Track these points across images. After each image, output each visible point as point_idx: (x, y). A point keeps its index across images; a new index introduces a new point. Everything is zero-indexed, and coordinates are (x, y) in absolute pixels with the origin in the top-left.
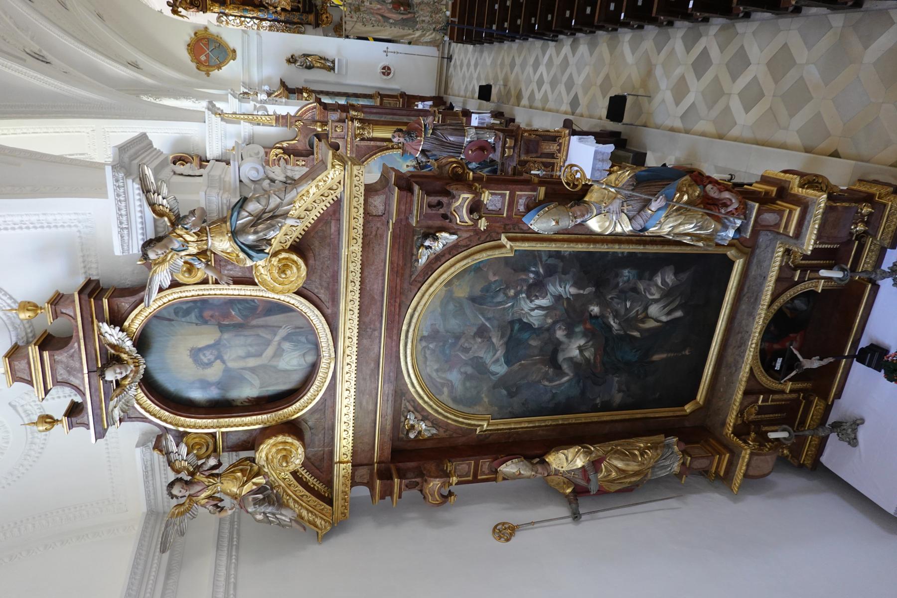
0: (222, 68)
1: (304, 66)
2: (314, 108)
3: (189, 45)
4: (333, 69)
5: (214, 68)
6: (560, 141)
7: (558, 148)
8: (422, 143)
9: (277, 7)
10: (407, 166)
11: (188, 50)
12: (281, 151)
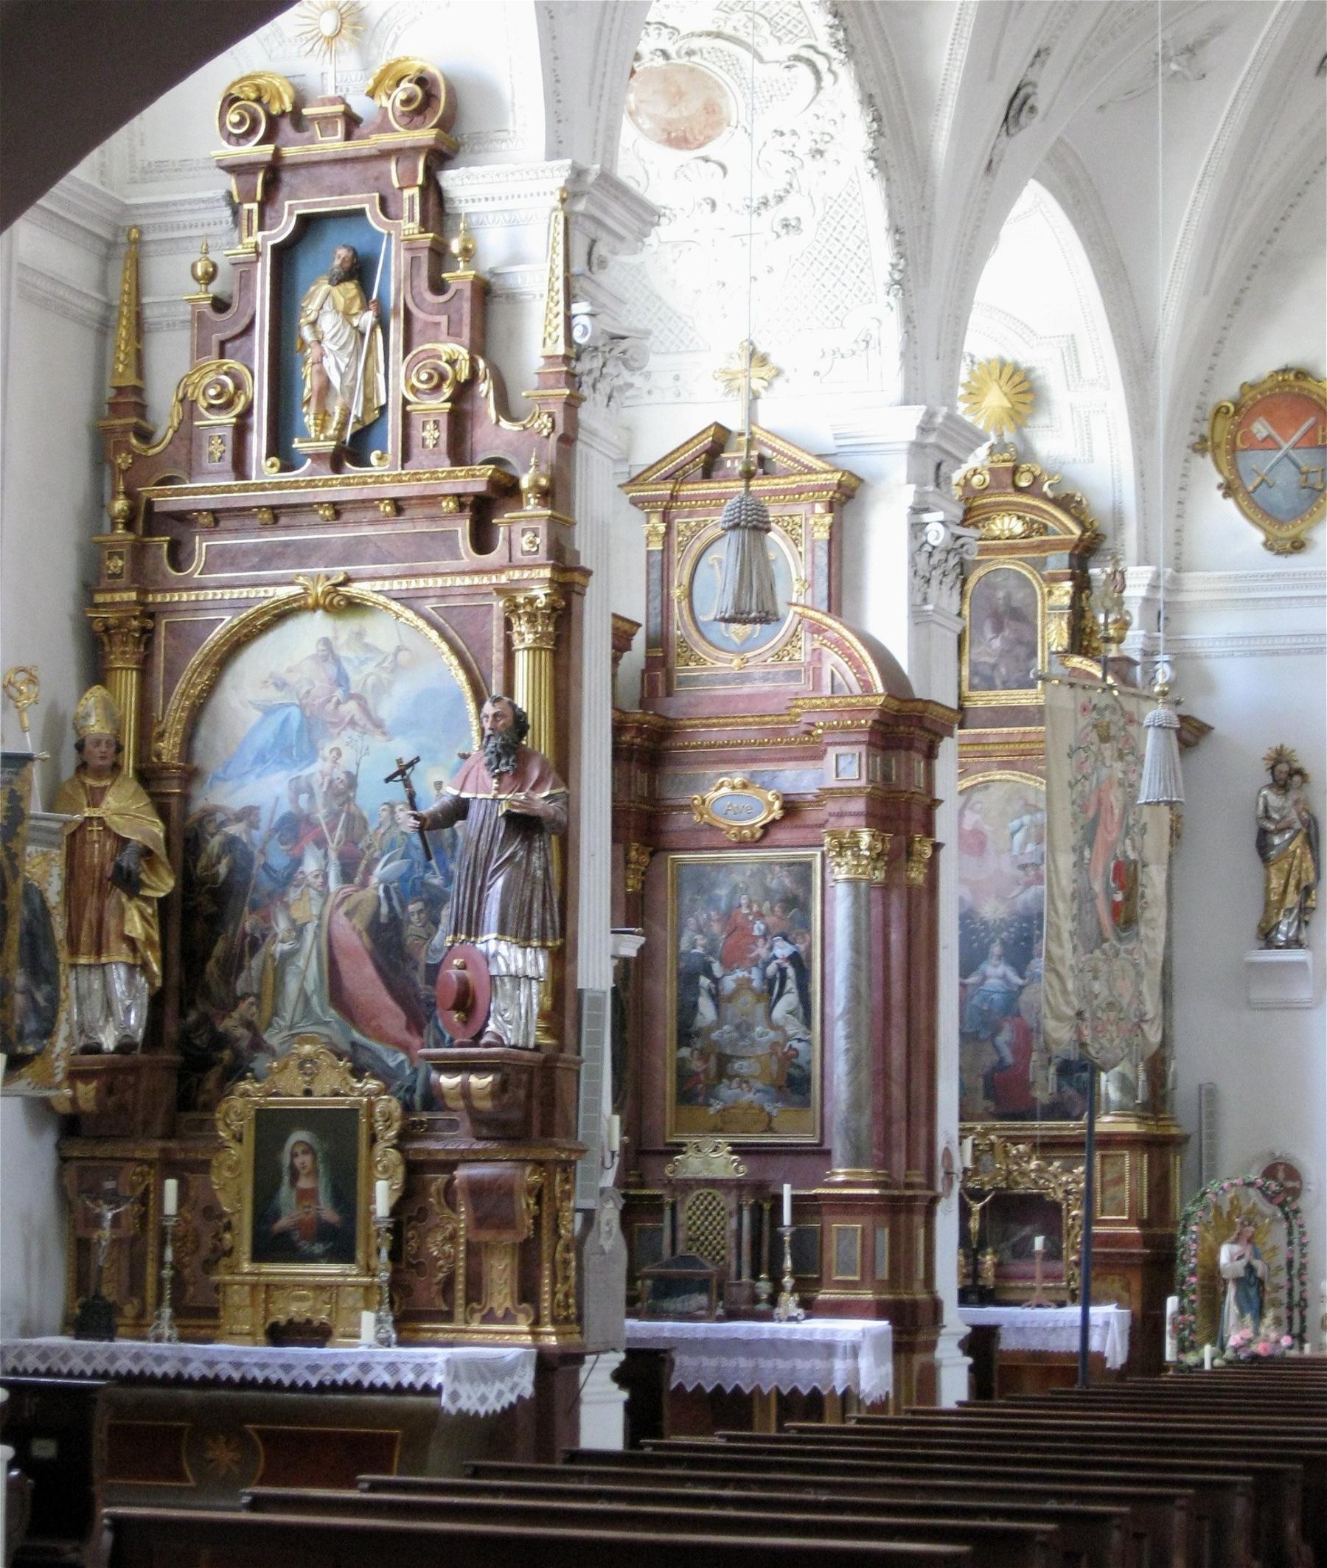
0: (1230, 503)
1: (1271, 827)
2: (867, 687)
3: (1301, 374)
4: (1267, 937)
5: (1226, 468)
6: (521, 1317)
7: (500, 1313)
8: (480, 796)
10: (439, 785)
11: (1285, 370)
12: (464, 375)
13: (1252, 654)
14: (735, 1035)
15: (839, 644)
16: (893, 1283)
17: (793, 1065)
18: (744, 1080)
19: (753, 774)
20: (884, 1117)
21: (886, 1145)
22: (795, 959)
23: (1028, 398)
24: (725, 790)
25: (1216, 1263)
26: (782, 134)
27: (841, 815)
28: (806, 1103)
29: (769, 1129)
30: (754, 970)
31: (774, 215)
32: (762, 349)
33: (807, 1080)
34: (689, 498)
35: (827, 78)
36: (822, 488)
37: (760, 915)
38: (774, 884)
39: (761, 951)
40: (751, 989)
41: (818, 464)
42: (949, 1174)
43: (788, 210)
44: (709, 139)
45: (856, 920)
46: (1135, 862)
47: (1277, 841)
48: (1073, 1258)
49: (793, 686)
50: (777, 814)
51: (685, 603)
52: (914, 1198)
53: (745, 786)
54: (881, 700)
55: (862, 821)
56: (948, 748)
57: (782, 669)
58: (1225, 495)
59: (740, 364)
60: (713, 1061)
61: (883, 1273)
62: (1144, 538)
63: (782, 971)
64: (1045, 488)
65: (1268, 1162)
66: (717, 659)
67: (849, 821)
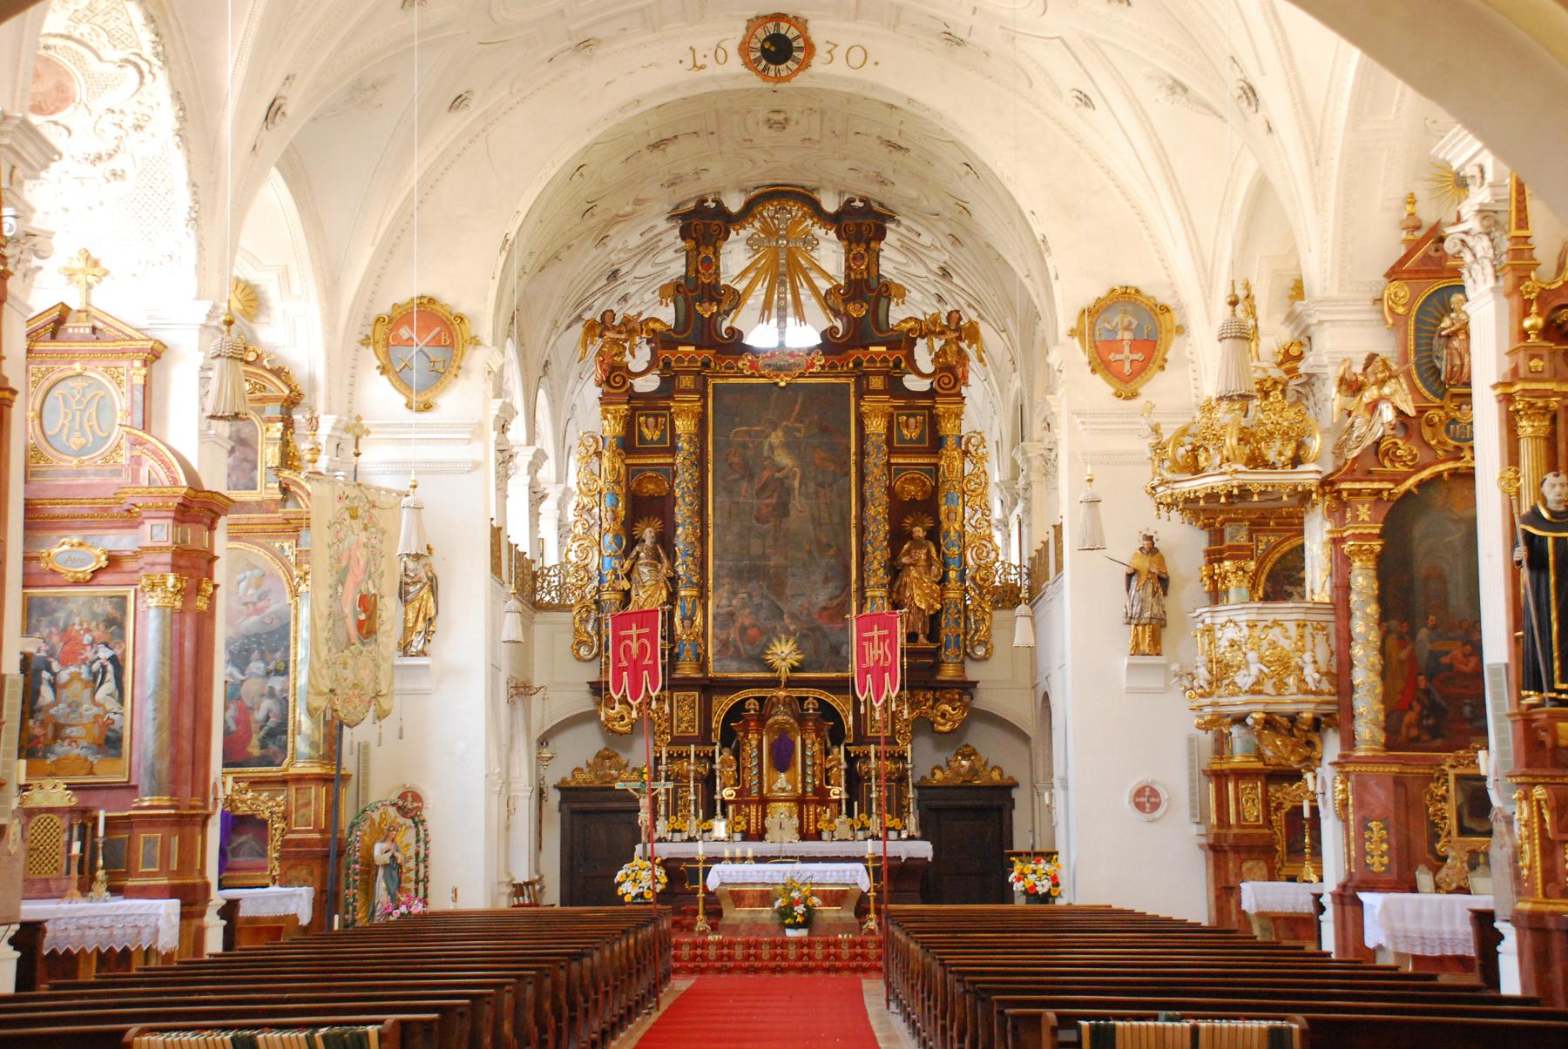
0: (384, 378)
2: (175, 481)
3: (431, 300)
9: (630, 580)
11: (422, 297)
13: (397, 473)
14: (68, 710)
15: (156, 453)
16: (179, 873)
17: (109, 730)
18: (73, 740)
19: (85, 536)
20: (175, 763)
21: (175, 780)
22: (113, 659)
23: (254, 304)
24: (66, 547)
25: (372, 855)
26: (113, 112)
27: (153, 564)
28: (119, 755)
29: (91, 772)
30: (83, 667)
31: (105, 167)
32: (94, 255)
33: (120, 740)
34: (41, 352)
35: (148, 77)
36: (139, 351)
37: (88, 630)
38: (99, 610)
39: (89, 654)
40: (81, 680)
41: (137, 335)
42: (215, 799)
43: (118, 163)
44: (58, 110)
45: (162, 632)
46: (375, 595)
47: (412, 589)
48: (275, 855)
49: (116, 480)
50: (103, 563)
51: (37, 422)
52: (197, 815)
53: (80, 544)
54: (185, 490)
55: (169, 568)
56: (222, 522)
57: (108, 468)
58: (381, 373)
59: (79, 264)
60: (50, 728)
61: (174, 866)
62: (329, 398)
63: (104, 667)
64: (265, 363)
65: (401, 791)
66: (61, 460)
67: (158, 569)
